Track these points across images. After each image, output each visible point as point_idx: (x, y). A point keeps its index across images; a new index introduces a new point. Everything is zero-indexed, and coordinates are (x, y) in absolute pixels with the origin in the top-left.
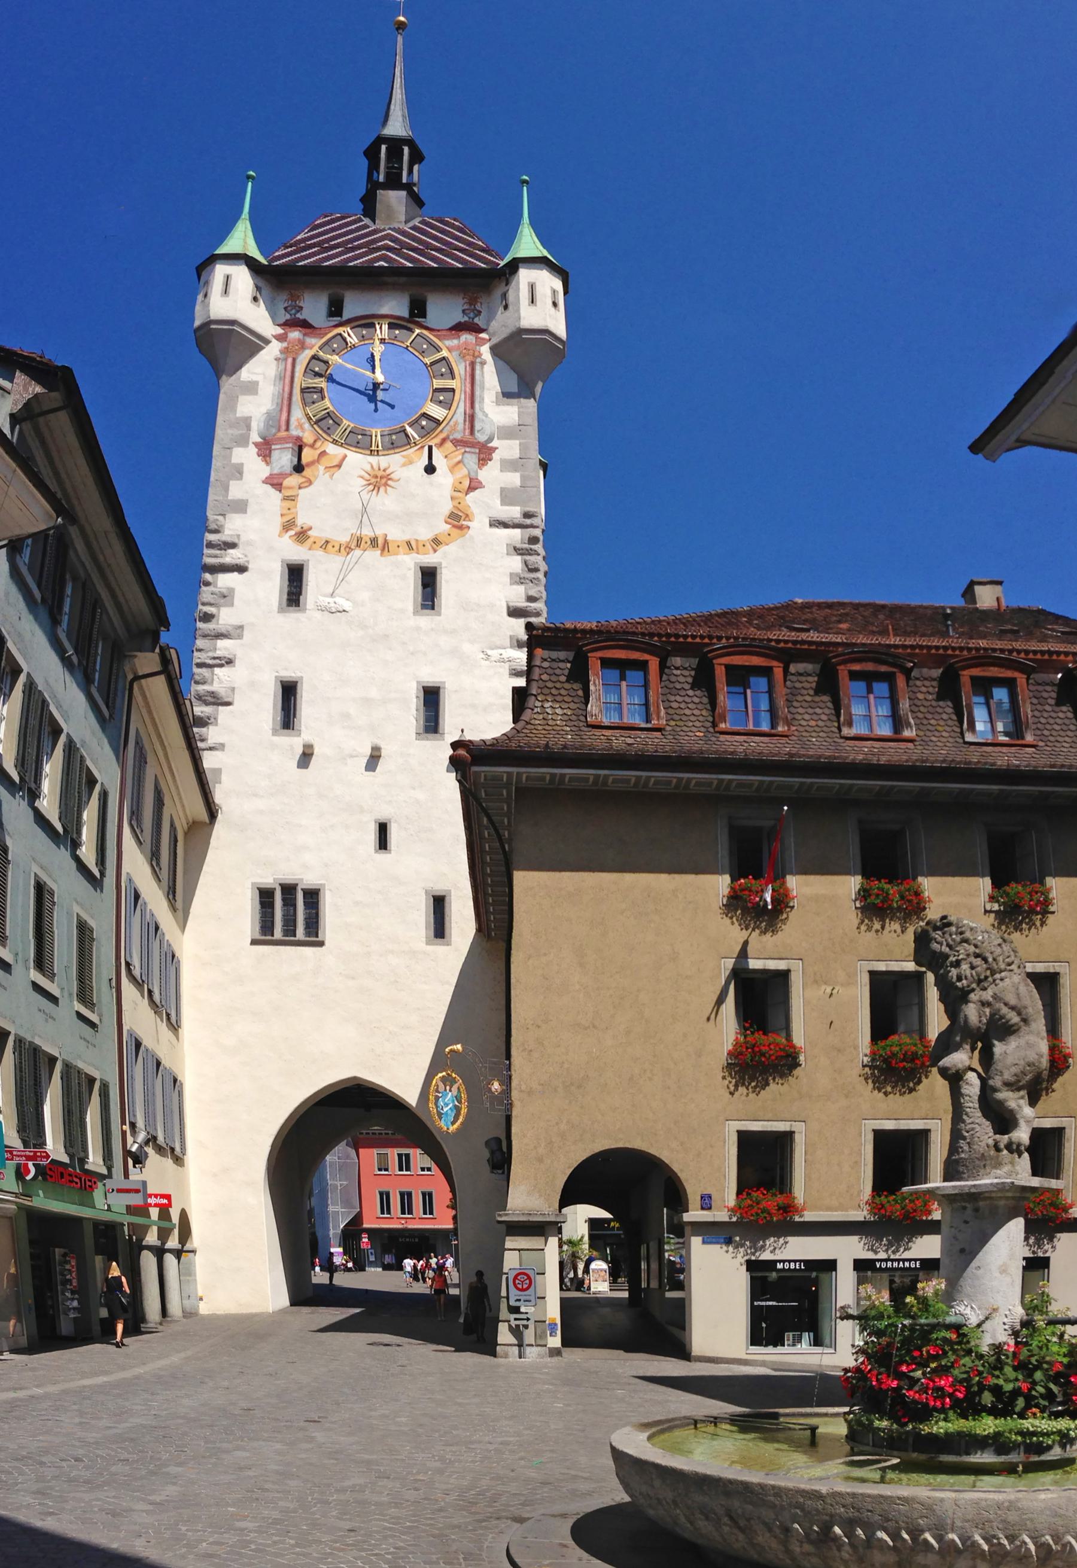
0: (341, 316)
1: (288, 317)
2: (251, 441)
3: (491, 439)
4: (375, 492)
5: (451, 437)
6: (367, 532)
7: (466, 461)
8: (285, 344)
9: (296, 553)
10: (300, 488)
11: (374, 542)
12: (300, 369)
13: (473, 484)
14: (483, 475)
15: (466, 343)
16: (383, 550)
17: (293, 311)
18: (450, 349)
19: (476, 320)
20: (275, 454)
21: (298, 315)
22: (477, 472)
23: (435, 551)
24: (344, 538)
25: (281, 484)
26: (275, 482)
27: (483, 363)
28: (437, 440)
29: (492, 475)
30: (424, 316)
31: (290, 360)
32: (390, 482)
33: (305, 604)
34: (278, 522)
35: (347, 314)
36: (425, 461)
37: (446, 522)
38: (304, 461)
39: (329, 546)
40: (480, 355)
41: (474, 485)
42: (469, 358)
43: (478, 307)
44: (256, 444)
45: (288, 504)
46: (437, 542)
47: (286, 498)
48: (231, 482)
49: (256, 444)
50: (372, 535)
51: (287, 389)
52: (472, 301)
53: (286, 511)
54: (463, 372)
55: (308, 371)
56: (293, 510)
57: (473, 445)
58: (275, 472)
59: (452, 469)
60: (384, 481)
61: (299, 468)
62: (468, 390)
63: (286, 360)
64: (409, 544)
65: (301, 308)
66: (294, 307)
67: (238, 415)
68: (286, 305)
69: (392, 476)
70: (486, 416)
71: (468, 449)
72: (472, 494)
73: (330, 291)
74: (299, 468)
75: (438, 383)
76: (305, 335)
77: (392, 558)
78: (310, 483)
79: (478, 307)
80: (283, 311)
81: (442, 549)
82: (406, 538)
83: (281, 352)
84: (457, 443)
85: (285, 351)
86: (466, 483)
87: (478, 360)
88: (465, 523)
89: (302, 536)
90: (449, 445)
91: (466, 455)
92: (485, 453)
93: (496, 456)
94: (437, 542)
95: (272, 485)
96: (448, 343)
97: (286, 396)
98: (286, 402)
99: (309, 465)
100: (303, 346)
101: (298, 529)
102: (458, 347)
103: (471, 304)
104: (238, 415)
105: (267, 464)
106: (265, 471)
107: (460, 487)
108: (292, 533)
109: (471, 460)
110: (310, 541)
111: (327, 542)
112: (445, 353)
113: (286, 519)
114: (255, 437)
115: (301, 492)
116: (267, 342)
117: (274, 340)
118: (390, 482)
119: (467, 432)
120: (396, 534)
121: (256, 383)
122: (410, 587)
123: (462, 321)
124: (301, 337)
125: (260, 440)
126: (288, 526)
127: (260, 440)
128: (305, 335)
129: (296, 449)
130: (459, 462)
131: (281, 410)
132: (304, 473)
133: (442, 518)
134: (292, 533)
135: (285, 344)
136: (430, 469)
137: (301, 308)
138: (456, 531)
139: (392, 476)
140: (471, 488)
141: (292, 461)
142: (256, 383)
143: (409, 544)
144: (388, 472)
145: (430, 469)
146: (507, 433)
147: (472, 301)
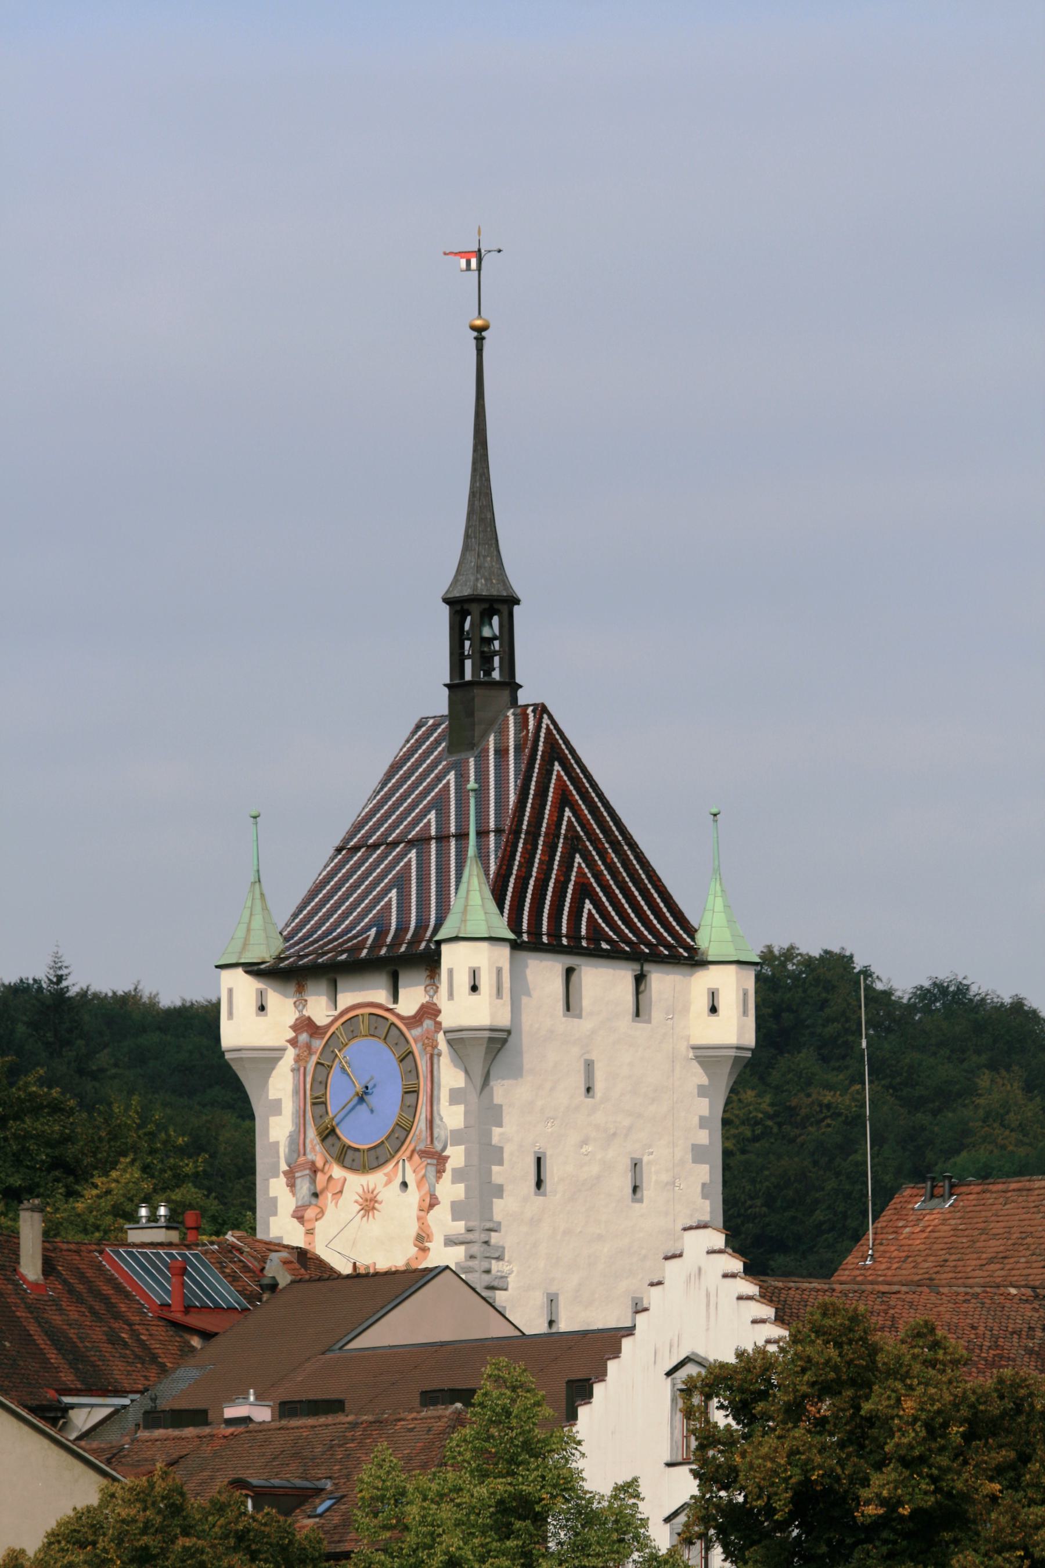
3: (444, 1148)
5: (418, 1148)
10: (317, 1220)
13: (433, 1201)
21: (305, 1012)
22: (434, 1187)
27: (439, 1055)
28: (408, 1153)
31: (302, 1069)
49: (285, 1173)
63: (299, 1070)
72: (431, 1212)
86: (428, 1200)
87: (436, 1051)
90: (416, 1157)
97: (302, 1113)
115: (317, 1224)
119: (429, 1142)
128: (311, 1036)
140: (431, 1206)
144: (375, 1193)
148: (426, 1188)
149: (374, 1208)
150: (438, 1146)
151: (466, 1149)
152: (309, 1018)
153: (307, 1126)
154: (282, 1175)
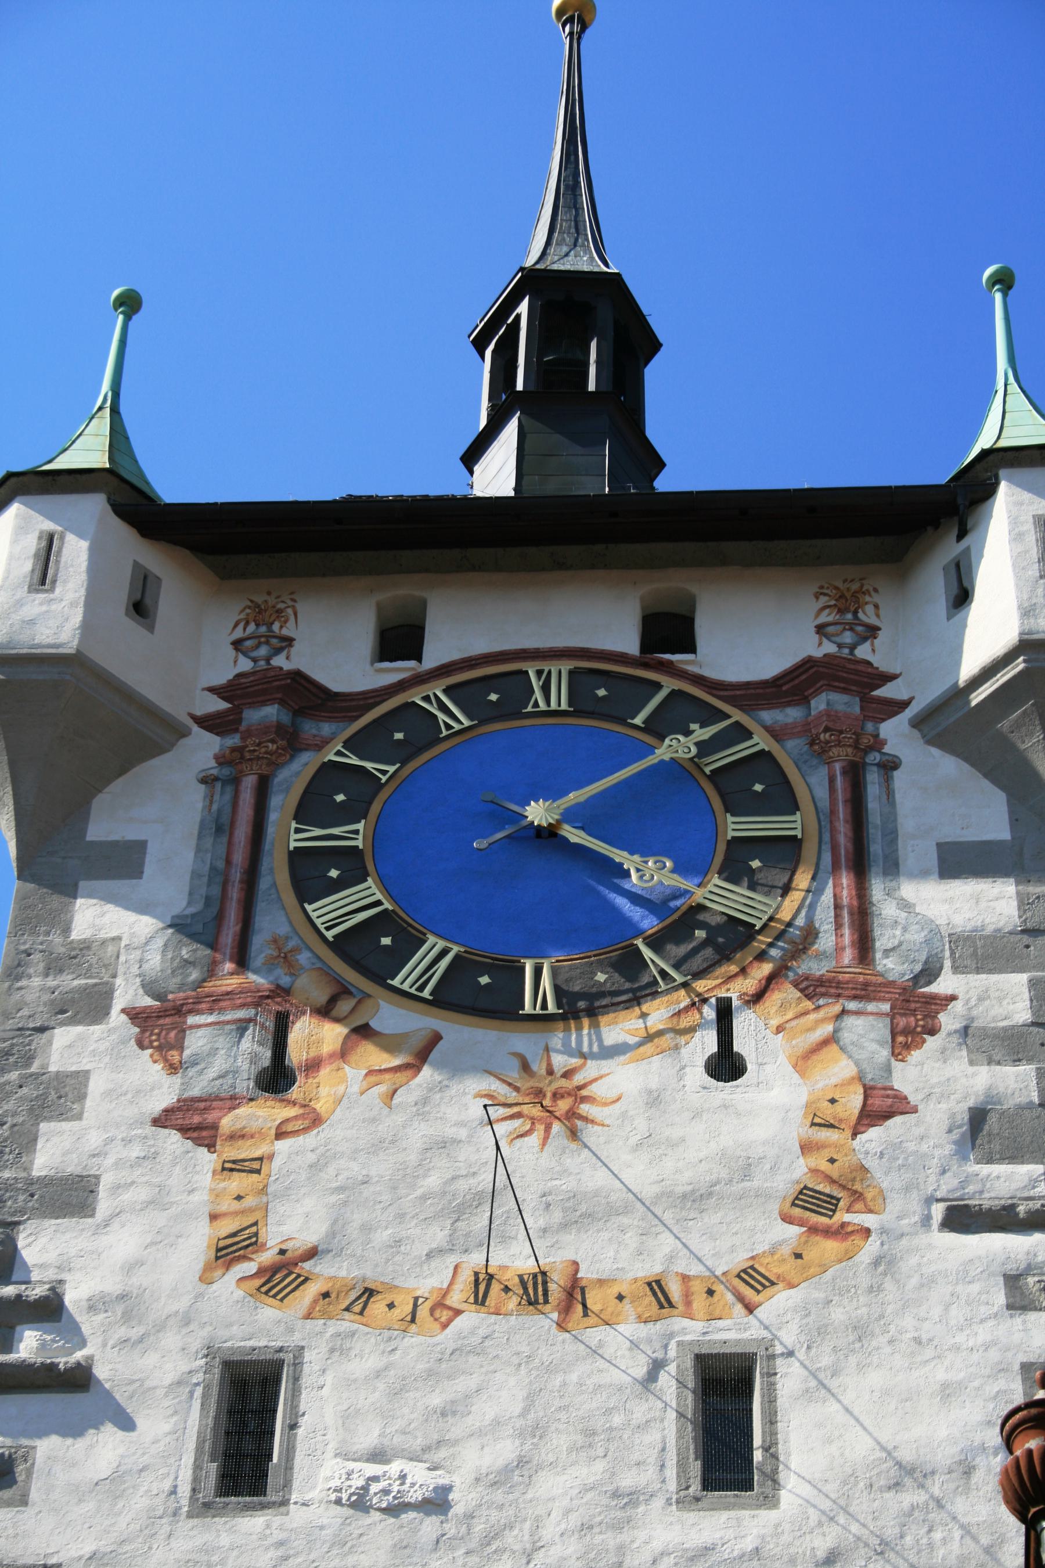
0: (419, 659)
1: (245, 665)
2: (119, 1003)
3: (930, 972)
4: (534, 1140)
6: (515, 1259)
7: (846, 1037)
8: (233, 740)
9: (259, 1326)
10: (280, 1135)
11: (534, 1290)
12: (282, 805)
13: (878, 1103)
14: (907, 1077)
15: (829, 714)
16: (566, 1310)
17: (263, 651)
18: (777, 734)
19: (863, 652)
20: (196, 1042)
22: (888, 1070)
23: (750, 1308)
24: (429, 1282)
25: (215, 1127)
26: (192, 1120)
27: (890, 766)
28: (749, 985)
29: (943, 1079)
30: (692, 649)
31: (249, 782)
32: (584, 1108)
33: (287, 1485)
34: (198, 1240)
35: (438, 649)
36: (708, 1042)
37: (787, 1219)
38: (296, 1053)
39: (378, 1307)
40: (878, 744)
41: (880, 1106)
42: (842, 755)
43: (867, 615)
44: (134, 1015)
45: (237, 1183)
46: (754, 1280)
47: (231, 1168)
48: (43, 1126)
49: (134, 1015)
50: (529, 1266)
51: (240, 857)
52: (847, 603)
53: (227, 1205)
54: (822, 793)
55: (307, 812)
56: (249, 1201)
57: (865, 992)
58: (195, 1092)
59: (805, 1060)
60: (563, 1106)
61: (276, 1078)
62: (844, 839)
63: (235, 781)
64: (656, 1287)
65: (289, 641)
66: (267, 639)
67: (75, 935)
68: (239, 633)
69: (593, 1090)
70: (906, 906)
71: (852, 1005)
72: (874, 1136)
73: (384, 596)
74: (276, 1078)
75: (735, 826)
76: (299, 713)
77: (596, 1335)
78: (316, 1121)
79: (867, 615)
80: (231, 652)
81: (777, 1304)
82: (652, 1268)
83: (221, 760)
84: (814, 989)
85: (232, 762)
86: (854, 1101)
87: (874, 757)
88: (847, 1217)
89: (281, 1276)
91: (849, 1021)
92: (914, 1014)
93: (948, 1020)
94: (754, 1280)
95: (184, 1130)
96: (767, 716)
97: (237, 875)
98: (235, 893)
99: (313, 1066)
100: (292, 743)
101: (267, 1257)
102: (805, 729)
103: (841, 611)
104: (75, 935)
105: (173, 1068)
106: (166, 1092)
107: (828, 1112)
108: (249, 1268)
109: (867, 1031)
110: (312, 1290)
111: (370, 1293)
112: (760, 741)
113: (227, 1226)
114: (127, 993)
115: (282, 1146)
116: (183, 733)
117: (195, 728)
118: (584, 1108)
119: (848, 956)
120: (608, 1256)
121: (141, 846)
122: (661, 1429)
123: (818, 653)
124: (286, 718)
125: (148, 1001)
126: (228, 1252)
127: (148, 1001)
128: (299, 713)
129: (270, 1024)
130: (825, 1042)
131: (220, 918)
132: (295, 1092)
133: (774, 1207)
134: (249, 1268)
135: (233, 740)
136: (726, 1066)
137: (289, 641)
138: (831, 1246)
139: (593, 1090)
141: (254, 1058)
142: (141, 846)
143: (656, 1287)
144: (579, 1079)
145: (726, 1066)
146: (984, 953)
147: (847, 603)
148: (838, 1069)
149: (572, 1114)
150: (891, 966)
151: (1033, 984)
152: (298, 676)
153: (261, 906)
154: (116, 1018)
